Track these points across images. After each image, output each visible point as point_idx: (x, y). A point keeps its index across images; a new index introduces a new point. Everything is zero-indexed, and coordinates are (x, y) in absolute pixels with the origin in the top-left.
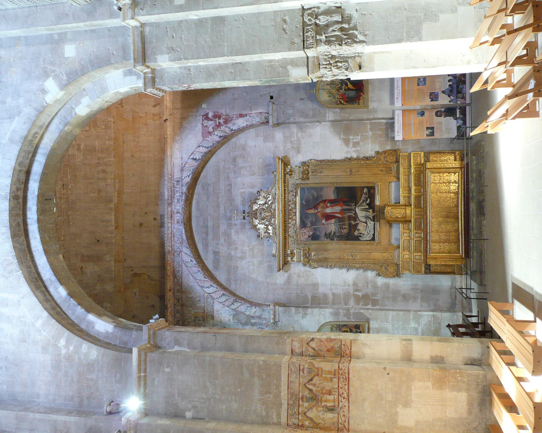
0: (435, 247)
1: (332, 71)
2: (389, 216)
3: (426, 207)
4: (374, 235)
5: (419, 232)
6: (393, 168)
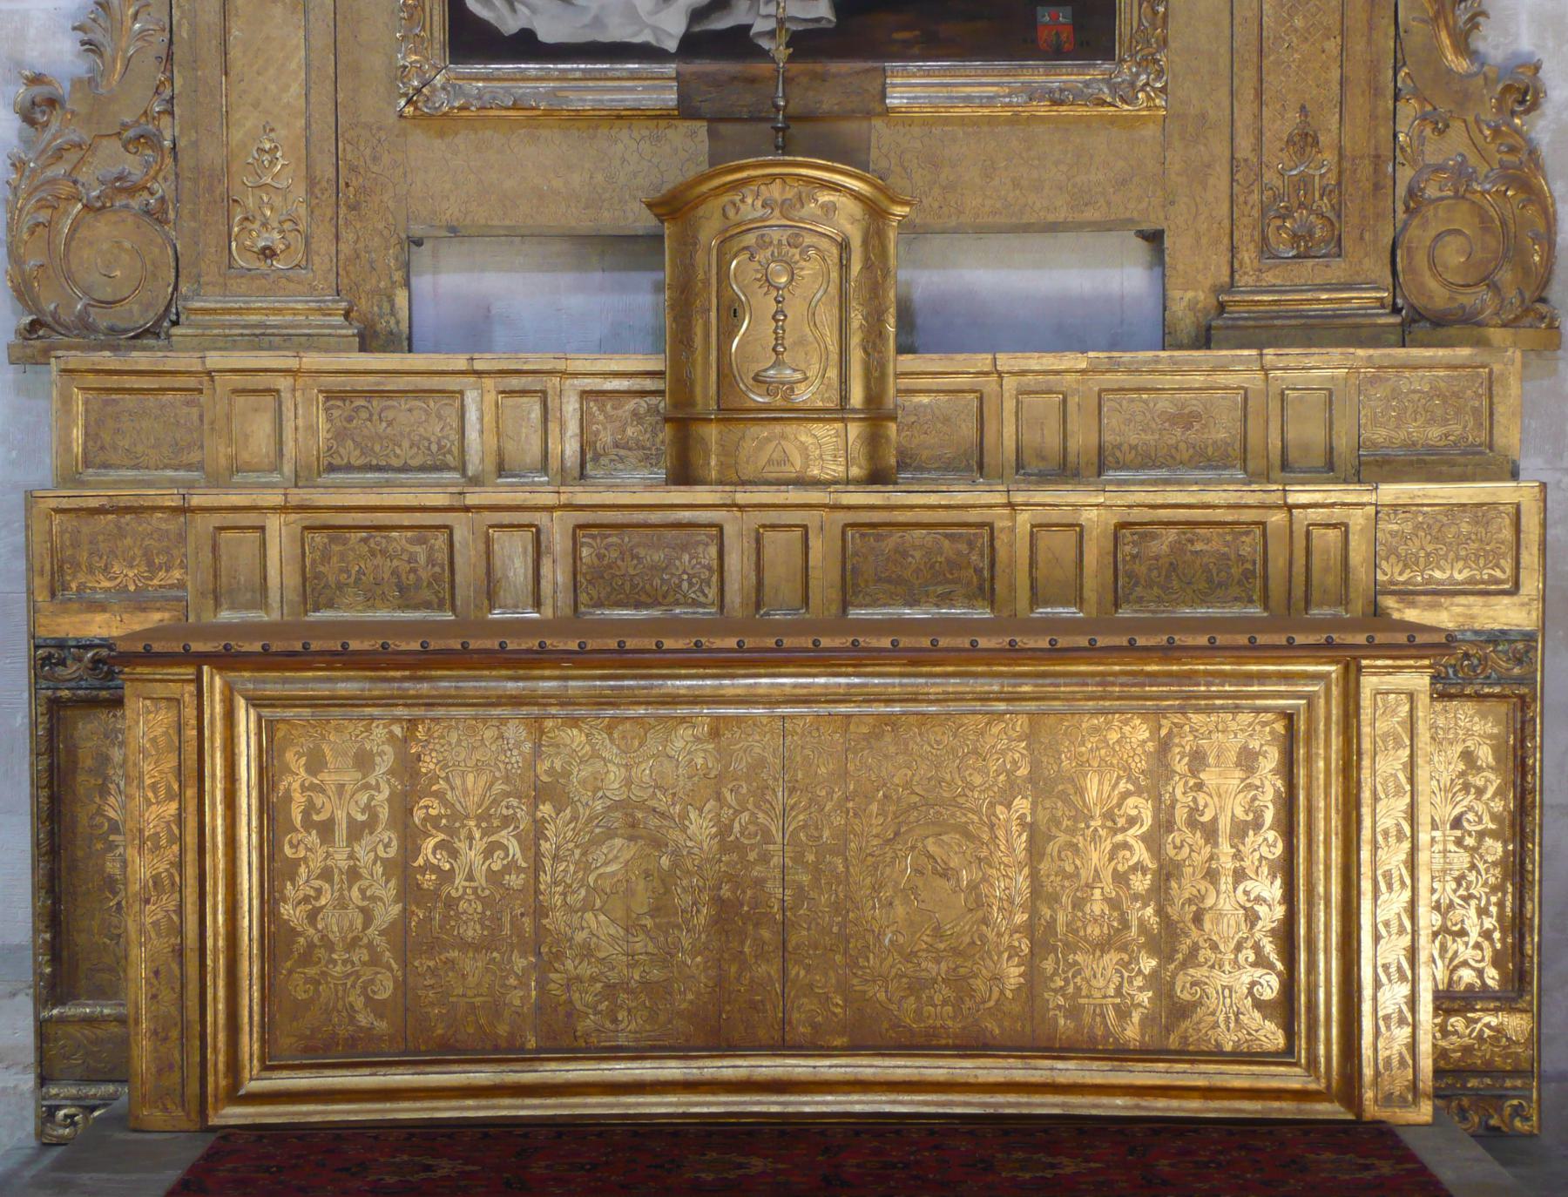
0: (346, 770)
2: (750, 207)
3: (857, 658)
4: (526, 46)
5: (556, 574)
6: (1337, 270)
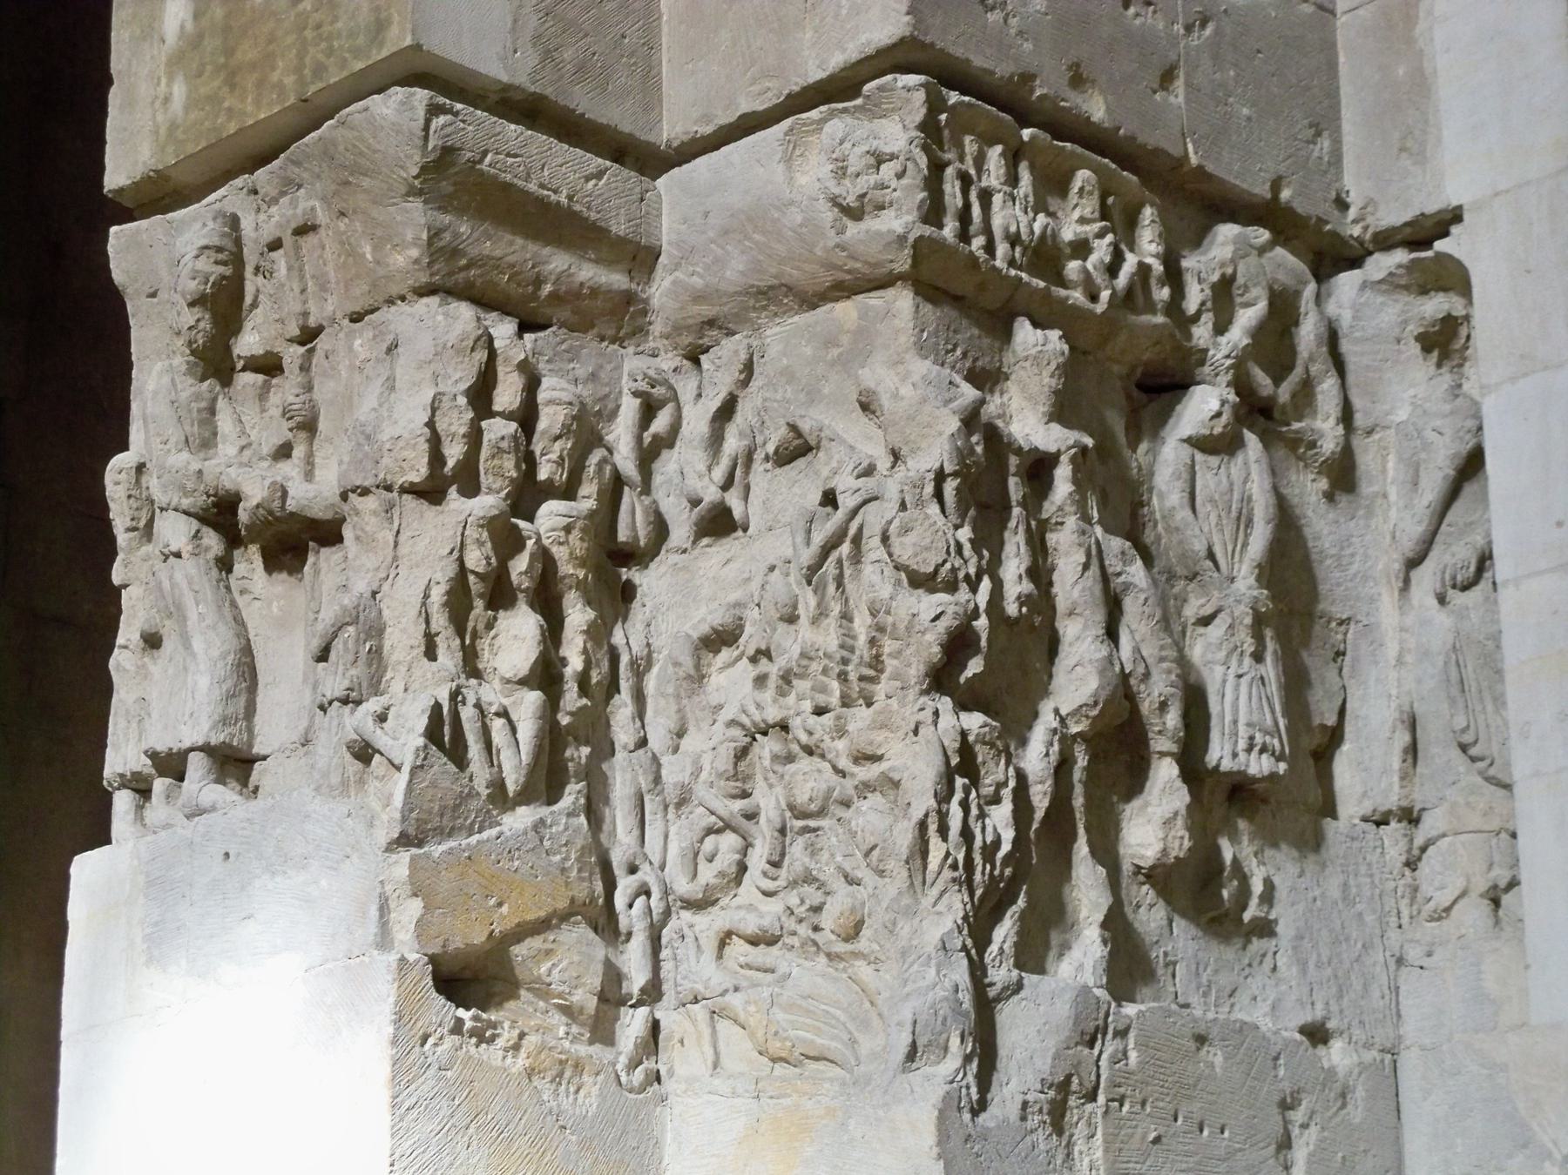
1: (431, 492)
